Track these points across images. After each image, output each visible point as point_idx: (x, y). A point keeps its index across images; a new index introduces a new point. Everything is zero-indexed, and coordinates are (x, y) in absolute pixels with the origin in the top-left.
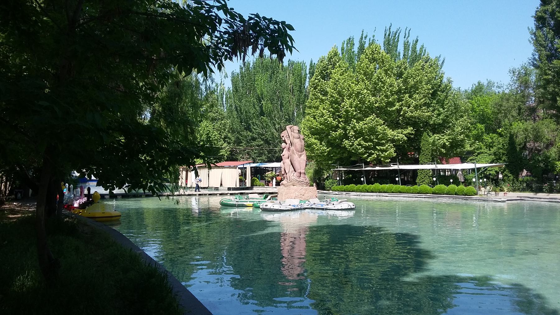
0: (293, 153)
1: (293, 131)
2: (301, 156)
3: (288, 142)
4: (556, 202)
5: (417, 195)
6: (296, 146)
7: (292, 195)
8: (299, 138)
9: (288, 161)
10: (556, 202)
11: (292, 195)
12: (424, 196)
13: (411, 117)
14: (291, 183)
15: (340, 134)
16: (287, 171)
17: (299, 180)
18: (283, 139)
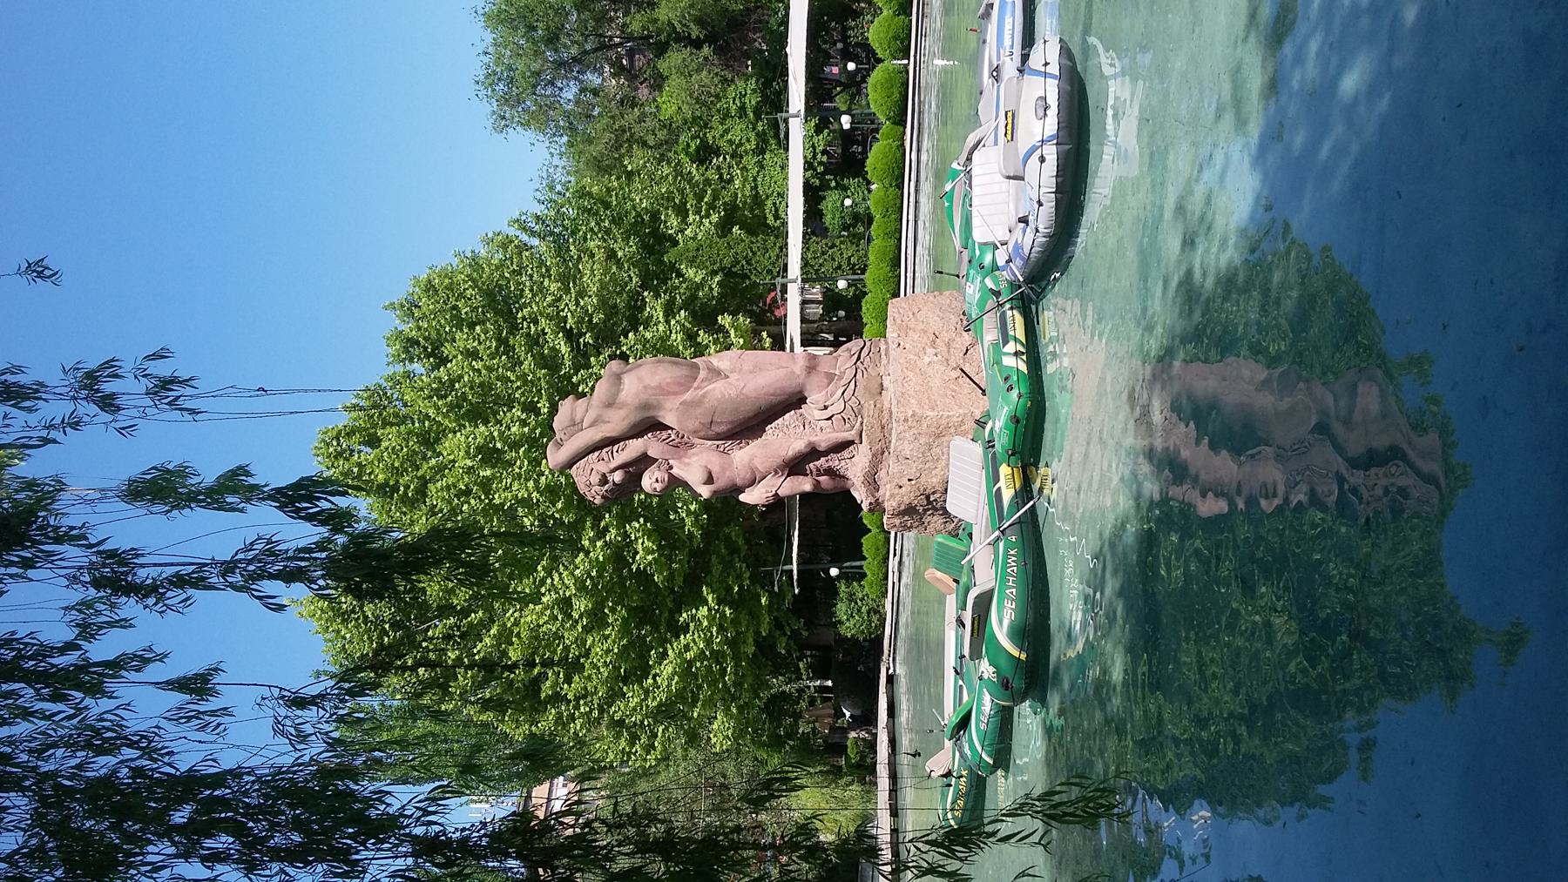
0: (697, 403)
1: (575, 426)
2: (716, 373)
3: (633, 448)
5: (909, 187)
6: (664, 391)
7: (936, 382)
8: (618, 378)
9: (746, 456)
11: (936, 382)
12: (911, 156)
13: (603, 303)
14: (869, 407)
15: (649, 534)
16: (798, 445)
17: (850, 374)
18: (617, 477)
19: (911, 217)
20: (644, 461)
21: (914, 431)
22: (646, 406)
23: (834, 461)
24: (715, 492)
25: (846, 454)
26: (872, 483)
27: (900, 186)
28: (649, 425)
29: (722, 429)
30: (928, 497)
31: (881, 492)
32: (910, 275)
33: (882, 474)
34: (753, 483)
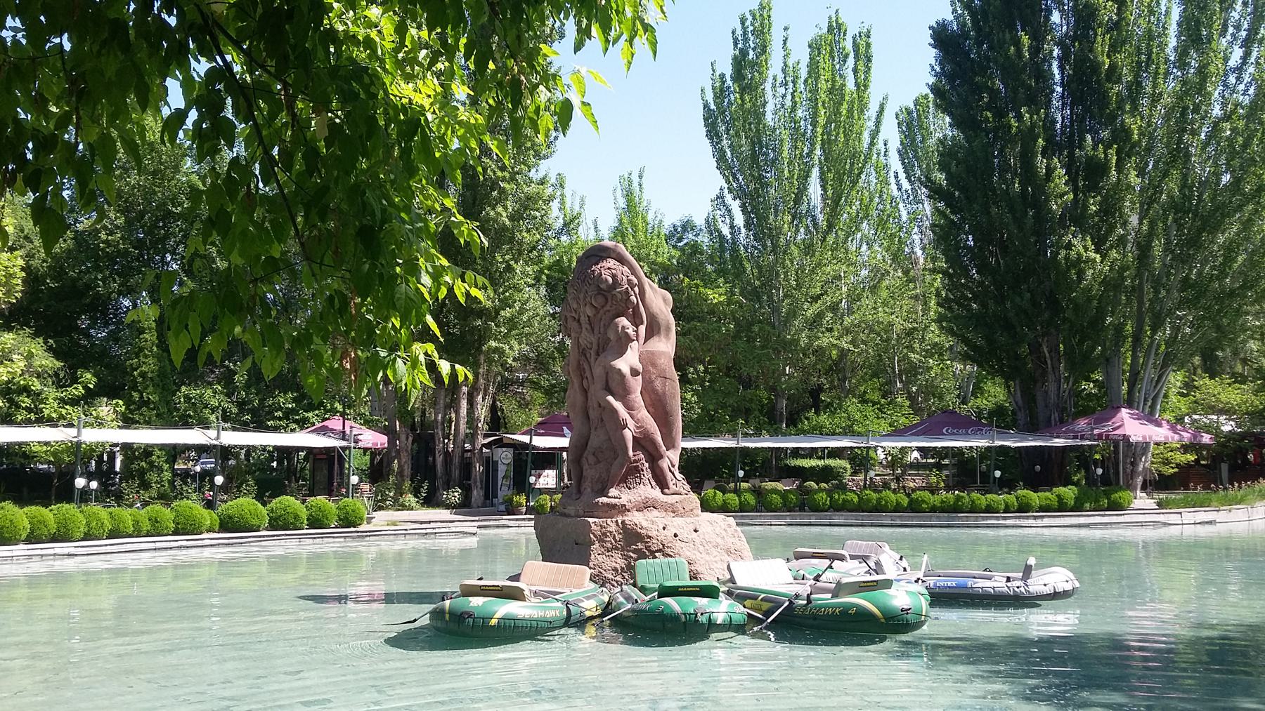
4: (498, 527)
5: (182, 540)
10: (498, 527)
19: (159, 545)
20: (636, 321)
21: (724, 533)
22: (668, 329)
23: (648, 475)
24: (622, 376)
25: (654, 483)
26: (646, 506)
27: (176, 533)
28: (654, 329)
29: (658, 384)
30: (659, 551)
31: (636, 513)
32: (109, 549)
33: (655, 513)
34: (629, 408)
